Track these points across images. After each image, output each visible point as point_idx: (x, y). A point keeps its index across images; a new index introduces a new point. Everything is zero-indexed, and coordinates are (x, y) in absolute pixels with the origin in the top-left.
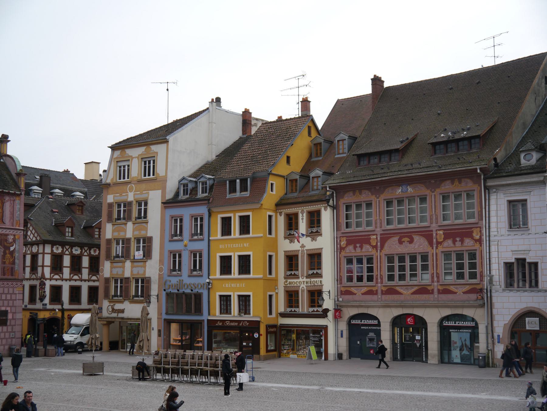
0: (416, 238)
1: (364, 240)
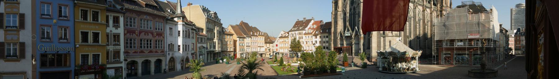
0: (149, 34)
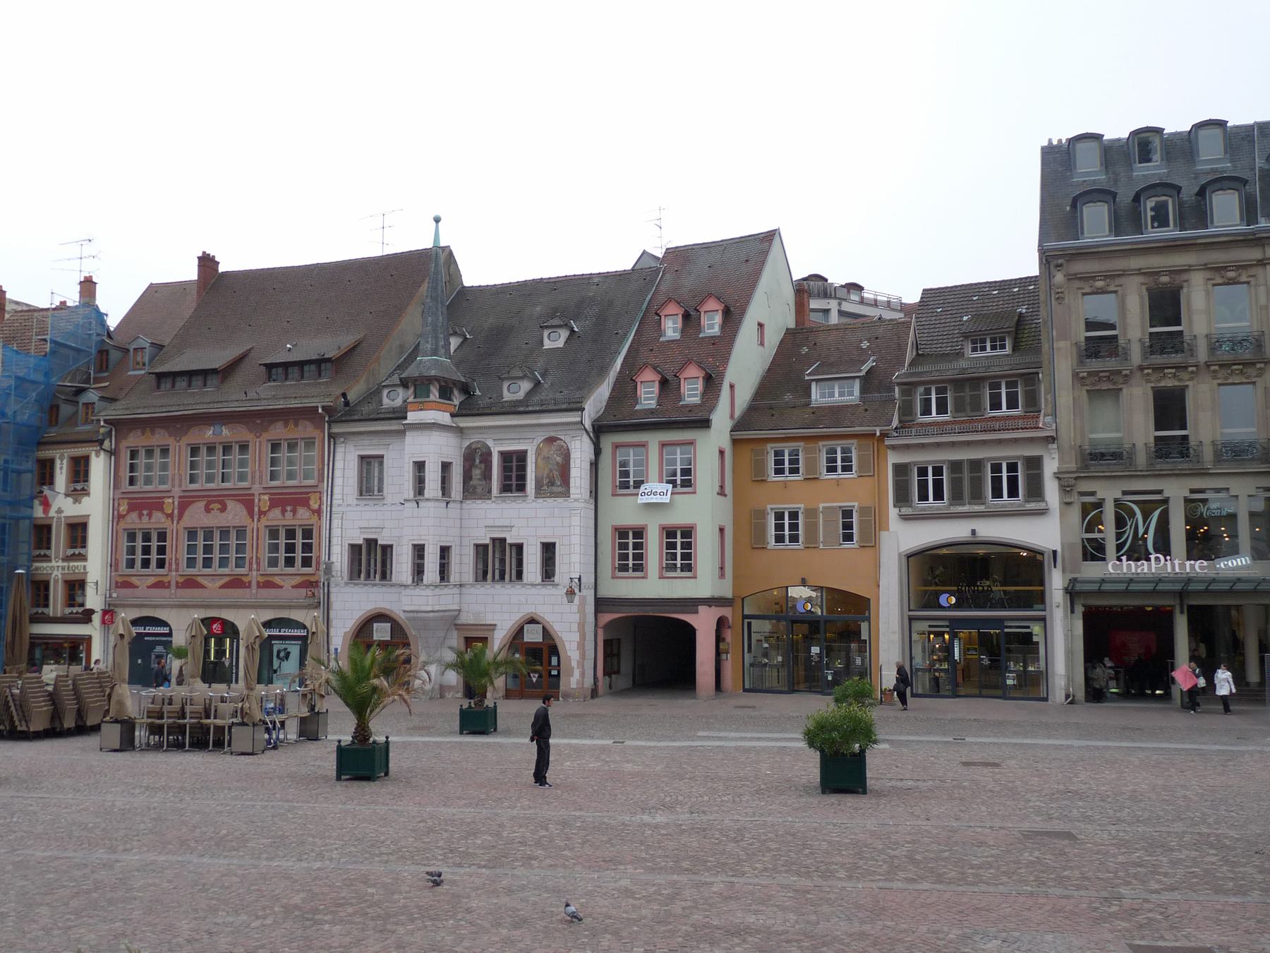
0: (231, 504)
1: (154, 505)
